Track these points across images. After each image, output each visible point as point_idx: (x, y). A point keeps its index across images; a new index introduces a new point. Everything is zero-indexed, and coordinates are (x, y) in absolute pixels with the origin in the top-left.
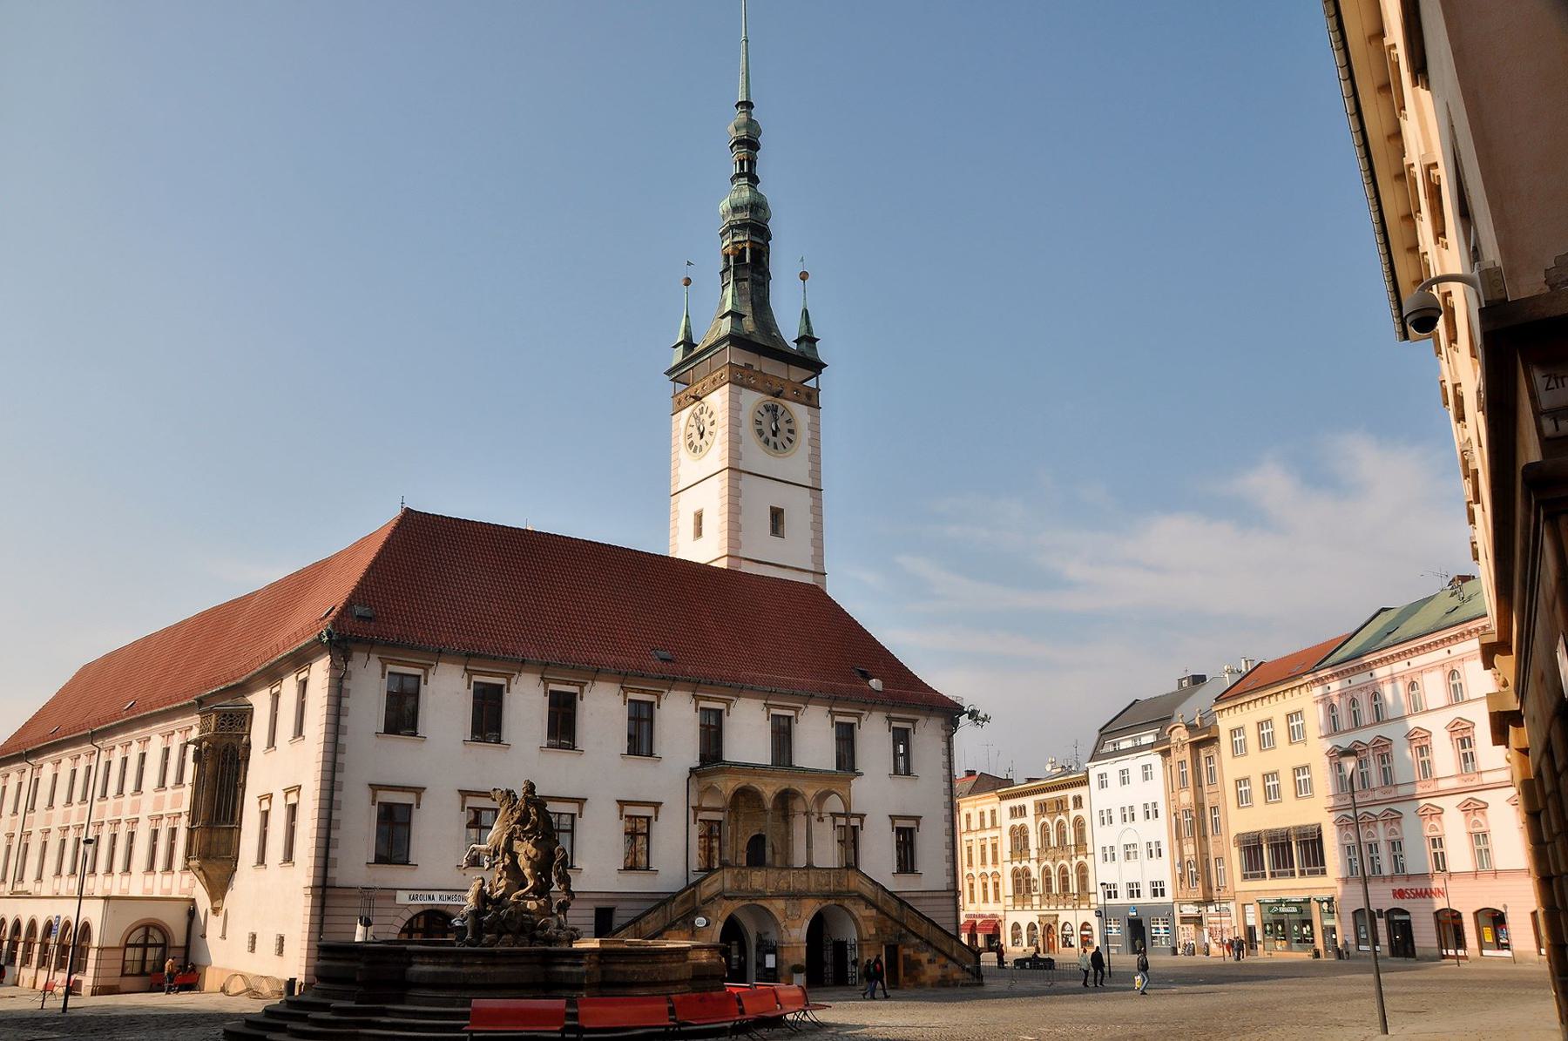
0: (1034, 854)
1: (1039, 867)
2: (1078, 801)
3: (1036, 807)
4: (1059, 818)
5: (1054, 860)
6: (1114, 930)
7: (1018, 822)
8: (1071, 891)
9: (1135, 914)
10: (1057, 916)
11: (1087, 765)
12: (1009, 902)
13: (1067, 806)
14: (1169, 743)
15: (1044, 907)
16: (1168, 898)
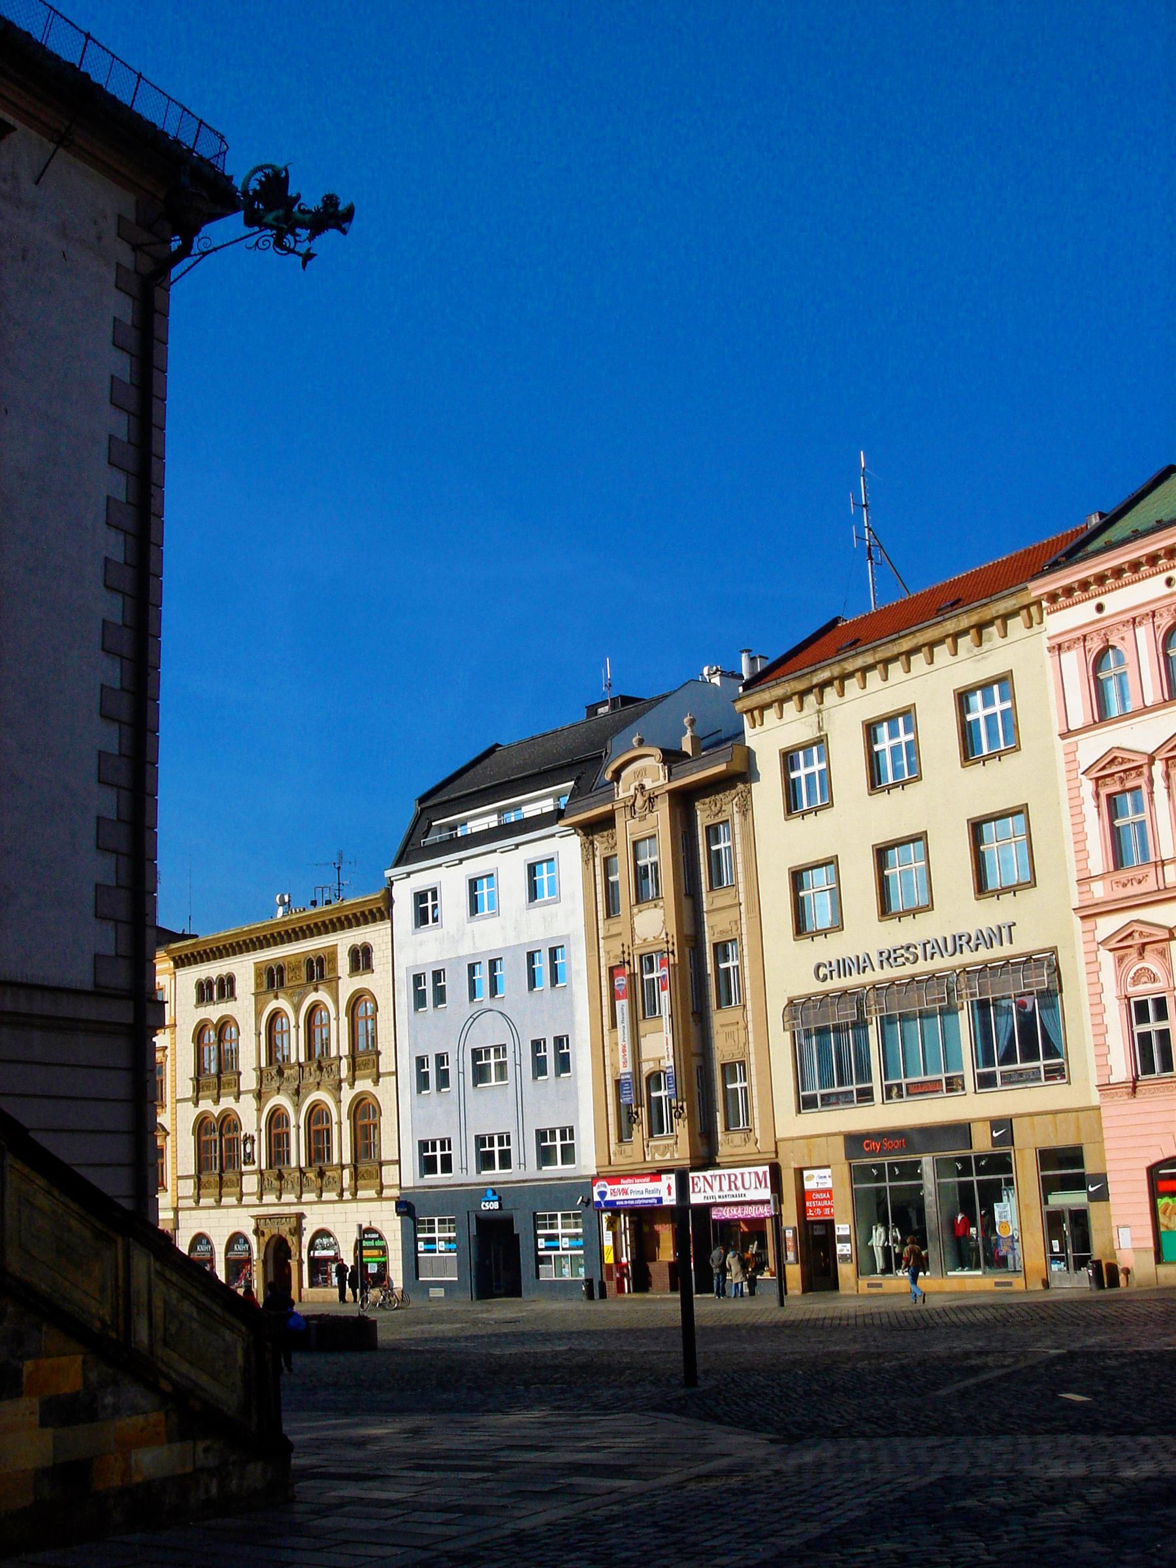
0: (249, 1081)
1: (259, 1110)
2: (361, 959)
3: (258, 975)
4: (312, 997)
5: (297, 1092)
6: (441, 1246)
7: (214, 1012)
8: (336, 1160)
9: (496, 1205)
10: (300, 1217)
11: (388, 873)
12: (188, 1187)
13: (334, 969)
14: (611, 799)
15: (270, 1198)
16: (587, 1162)
